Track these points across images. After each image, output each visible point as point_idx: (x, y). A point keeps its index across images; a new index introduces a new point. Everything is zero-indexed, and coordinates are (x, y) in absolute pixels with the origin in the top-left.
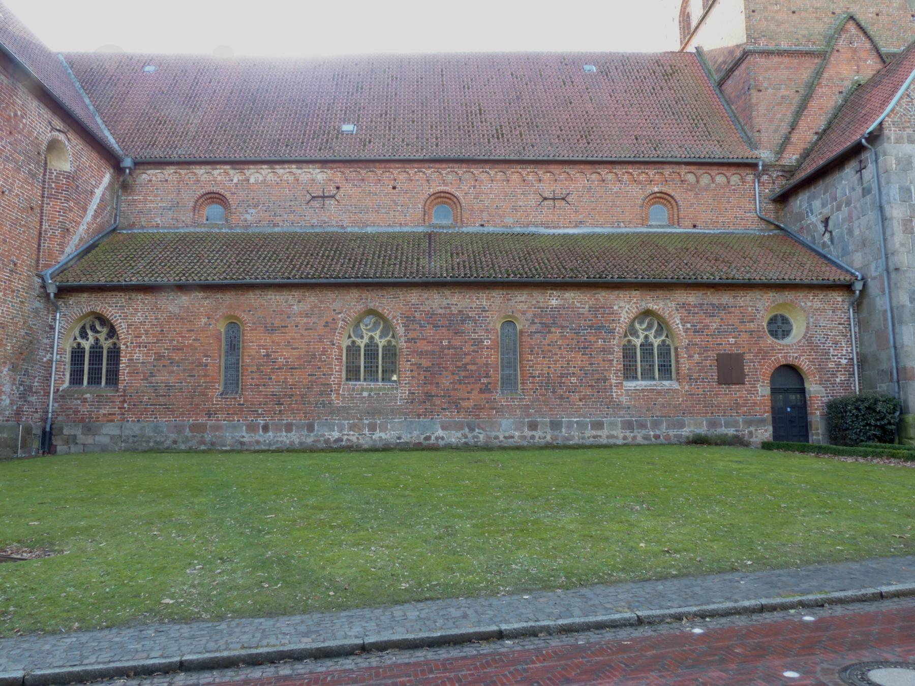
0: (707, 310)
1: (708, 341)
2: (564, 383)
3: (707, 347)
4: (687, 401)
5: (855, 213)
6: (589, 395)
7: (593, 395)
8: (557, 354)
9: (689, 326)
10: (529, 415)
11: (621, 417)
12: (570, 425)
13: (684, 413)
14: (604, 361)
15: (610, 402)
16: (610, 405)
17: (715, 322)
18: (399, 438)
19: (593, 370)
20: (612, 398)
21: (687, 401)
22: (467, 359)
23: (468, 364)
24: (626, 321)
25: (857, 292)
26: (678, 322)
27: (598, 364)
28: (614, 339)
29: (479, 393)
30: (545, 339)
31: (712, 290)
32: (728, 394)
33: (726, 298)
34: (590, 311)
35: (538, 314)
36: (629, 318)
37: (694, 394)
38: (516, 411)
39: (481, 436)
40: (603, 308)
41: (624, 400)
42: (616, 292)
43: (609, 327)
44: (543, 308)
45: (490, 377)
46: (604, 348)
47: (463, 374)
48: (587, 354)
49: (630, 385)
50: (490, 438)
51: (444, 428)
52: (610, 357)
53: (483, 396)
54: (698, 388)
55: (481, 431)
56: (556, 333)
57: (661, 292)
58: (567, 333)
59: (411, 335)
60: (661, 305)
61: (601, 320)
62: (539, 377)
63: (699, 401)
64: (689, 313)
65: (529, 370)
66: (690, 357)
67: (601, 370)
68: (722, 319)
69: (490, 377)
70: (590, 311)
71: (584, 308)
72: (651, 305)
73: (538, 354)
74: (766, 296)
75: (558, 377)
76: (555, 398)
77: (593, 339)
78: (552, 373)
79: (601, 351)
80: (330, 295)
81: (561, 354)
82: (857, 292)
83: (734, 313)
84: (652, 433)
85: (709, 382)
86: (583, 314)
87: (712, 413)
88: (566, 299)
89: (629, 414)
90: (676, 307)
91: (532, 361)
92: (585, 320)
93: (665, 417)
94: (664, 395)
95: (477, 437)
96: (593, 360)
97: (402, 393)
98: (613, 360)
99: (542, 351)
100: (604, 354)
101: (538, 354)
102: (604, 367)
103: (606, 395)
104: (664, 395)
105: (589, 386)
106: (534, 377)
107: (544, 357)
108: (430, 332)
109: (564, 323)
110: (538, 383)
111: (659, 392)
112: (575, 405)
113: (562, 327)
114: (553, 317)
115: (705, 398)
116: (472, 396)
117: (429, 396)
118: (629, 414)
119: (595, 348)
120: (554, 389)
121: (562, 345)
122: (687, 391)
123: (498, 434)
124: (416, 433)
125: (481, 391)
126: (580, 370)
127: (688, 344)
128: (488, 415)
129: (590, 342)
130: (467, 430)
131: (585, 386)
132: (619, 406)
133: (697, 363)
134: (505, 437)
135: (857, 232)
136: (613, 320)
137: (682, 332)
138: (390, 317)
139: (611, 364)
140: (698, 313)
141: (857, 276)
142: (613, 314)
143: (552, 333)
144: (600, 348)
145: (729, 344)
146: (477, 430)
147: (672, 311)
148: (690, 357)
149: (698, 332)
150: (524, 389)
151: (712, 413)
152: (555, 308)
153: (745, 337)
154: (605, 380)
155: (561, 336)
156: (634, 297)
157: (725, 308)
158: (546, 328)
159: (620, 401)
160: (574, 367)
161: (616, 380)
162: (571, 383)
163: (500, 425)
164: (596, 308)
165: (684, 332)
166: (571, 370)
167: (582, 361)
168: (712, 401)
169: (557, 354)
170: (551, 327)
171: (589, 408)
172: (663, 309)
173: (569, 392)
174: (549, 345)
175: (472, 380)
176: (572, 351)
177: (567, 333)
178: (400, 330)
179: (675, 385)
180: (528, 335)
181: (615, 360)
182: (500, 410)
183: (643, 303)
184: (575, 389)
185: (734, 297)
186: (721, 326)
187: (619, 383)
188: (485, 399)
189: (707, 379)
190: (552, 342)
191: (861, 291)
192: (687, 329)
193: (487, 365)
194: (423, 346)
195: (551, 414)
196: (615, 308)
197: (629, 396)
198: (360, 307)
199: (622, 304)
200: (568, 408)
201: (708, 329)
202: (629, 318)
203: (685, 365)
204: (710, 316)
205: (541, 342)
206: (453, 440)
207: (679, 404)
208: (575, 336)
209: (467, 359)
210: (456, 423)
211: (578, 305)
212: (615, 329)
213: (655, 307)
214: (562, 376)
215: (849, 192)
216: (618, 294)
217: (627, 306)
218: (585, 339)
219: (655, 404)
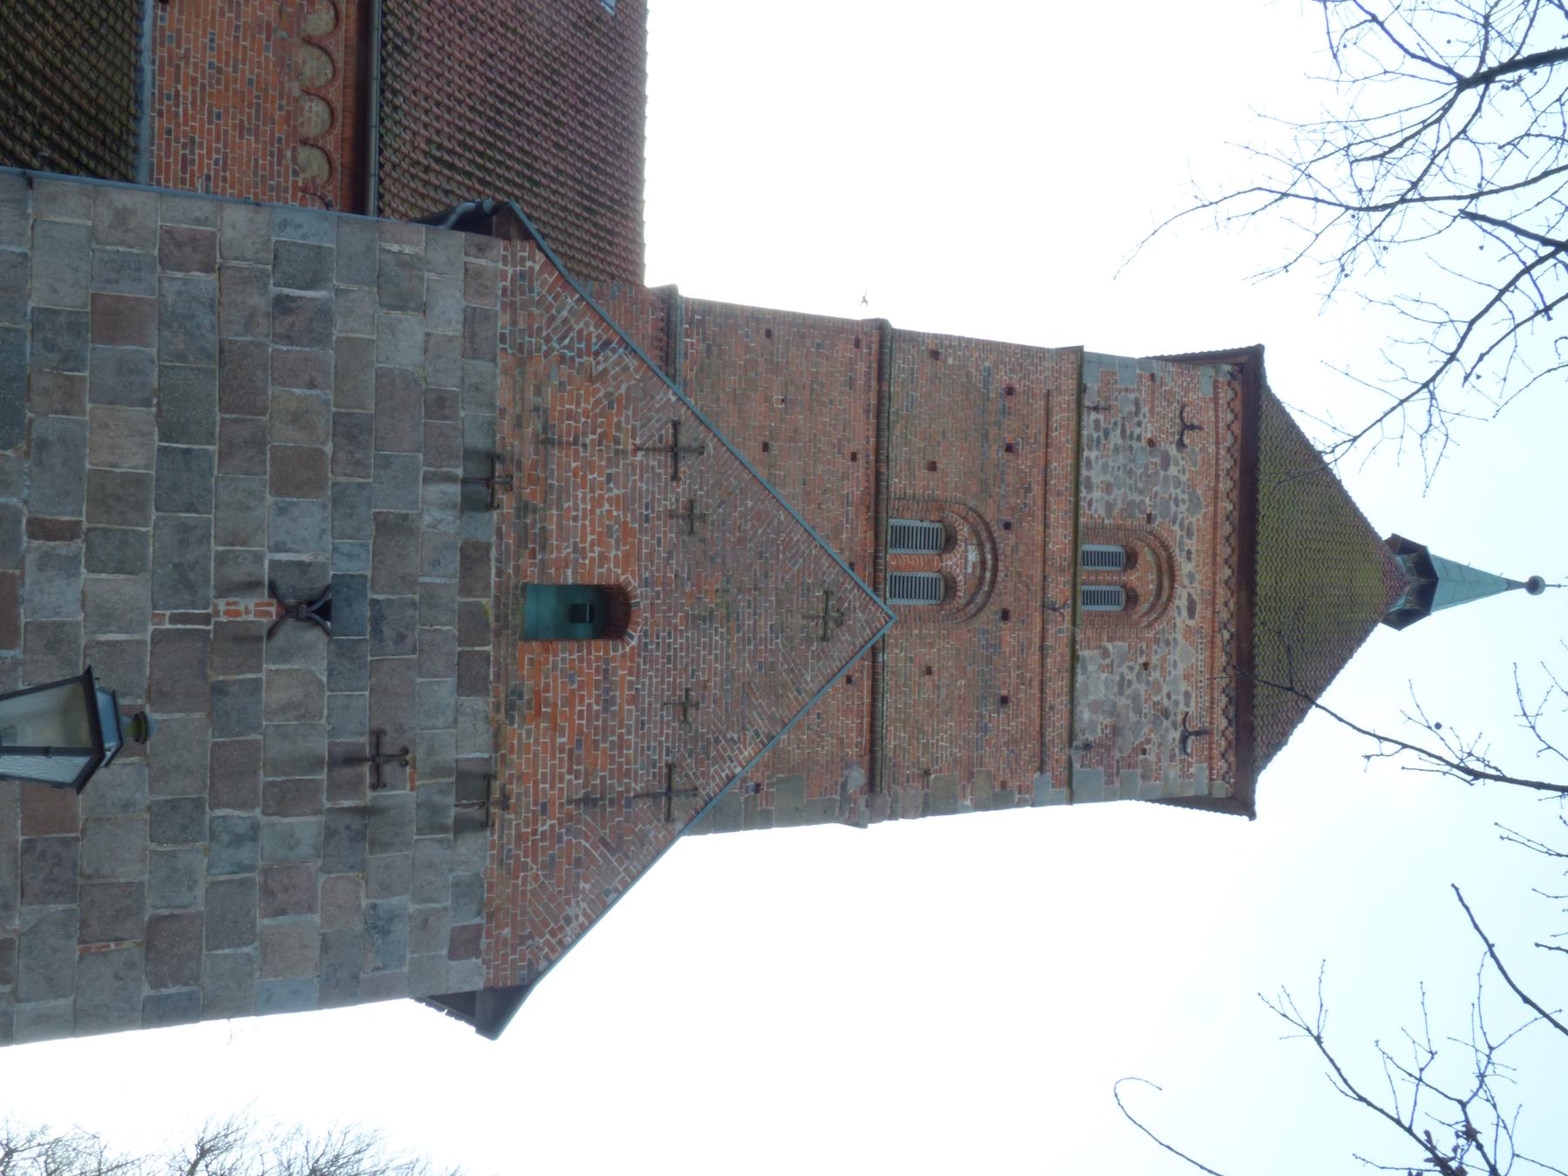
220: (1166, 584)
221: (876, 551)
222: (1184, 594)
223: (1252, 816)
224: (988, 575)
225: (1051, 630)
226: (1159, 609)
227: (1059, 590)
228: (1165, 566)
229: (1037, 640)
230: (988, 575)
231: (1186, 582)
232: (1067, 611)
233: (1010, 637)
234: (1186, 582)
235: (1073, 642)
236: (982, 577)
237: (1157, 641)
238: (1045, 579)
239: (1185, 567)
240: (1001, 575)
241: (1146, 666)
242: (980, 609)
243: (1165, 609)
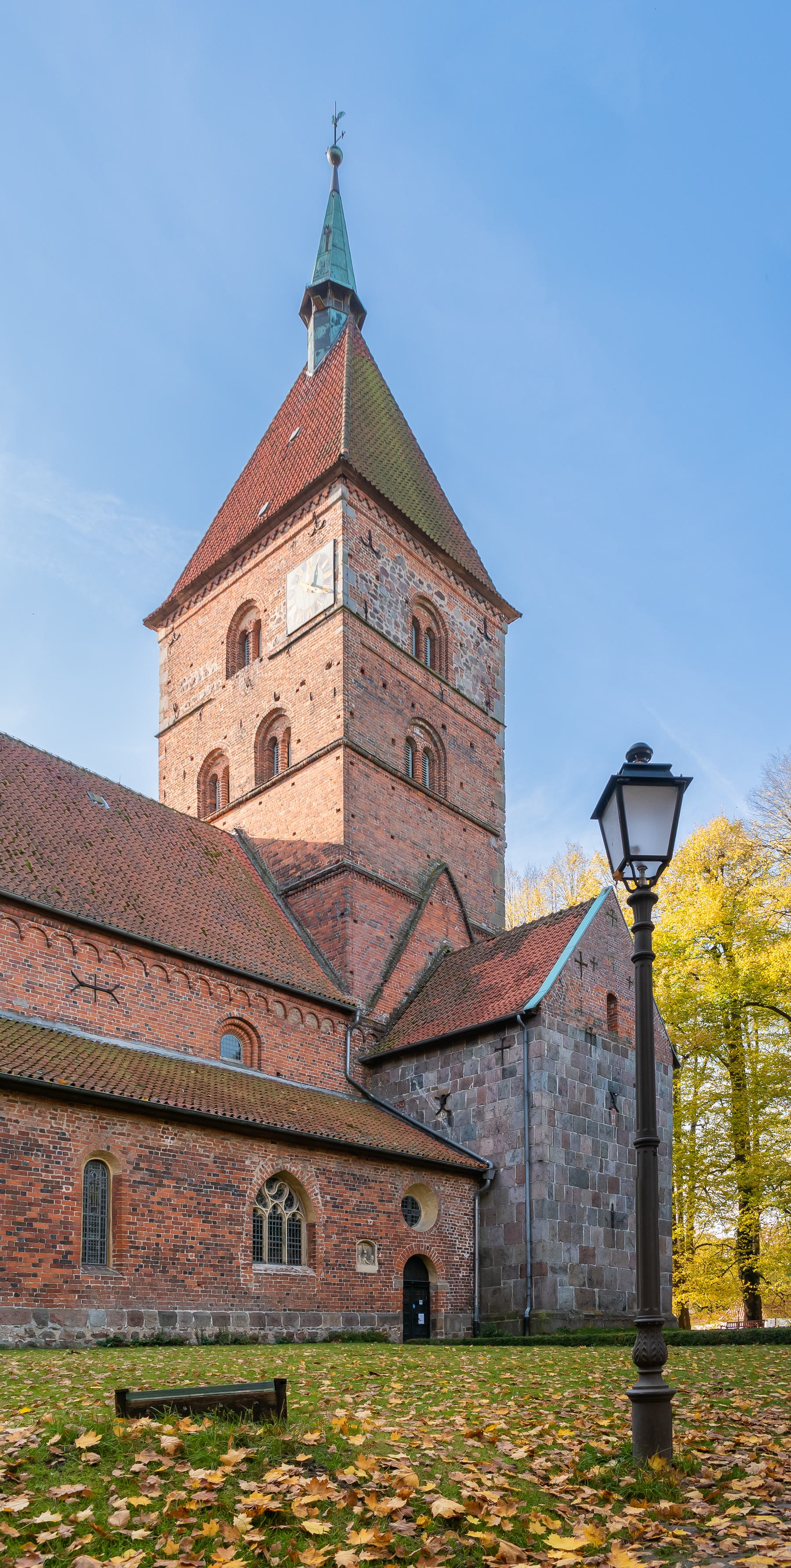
0: (347, 1181)
1: (347, 1220)
2: (178, 1259)
3: (345, 1227)
4: (322, 1291)
5: (489, 1095)
6: (210, 1278)
7: (215, 1279)
8: (170, 1218)
9: (328, 1198)
10: (128, 1304)
11: (248, 1310)
12: (186, 1319)
13: (318, 1307)
14: (230, 1233)
15: (236, 1289)
16: (236, 1293)
17: (355, 1198)
19: (216, 1245)
20: (239, 1284)
21: (322, 1291)
22: (34, 1213)
23: (35, 1220)
24: (259, 1182)
25: (489, 1181)
26: (317, 1191)
27: (223, 1236)
28: (244, 1204)
29: (52, 1266)
30: (153, 1194)
31: (354, 1157)
32: (363, 1285)
33: (367, 1170)
34: (215, 1162)
35: (146, 1156)
36: (263, 1178)
37: (330, 1284)
38: (109, 1297)
39: (57, 1334)
40: (233, 1160)
41: (253, 1286)
42: (250, 1142)
43: (238, 1187)
44: (153, 1148)
45: (71, 1243)
46: (230, 1216)
48: (209, 1222)
49: (259, 1267)
50: (69, 1335)
52: (238, 1228)
54: (334, 1277)
55: (57, 1326)
56: (169, 1186)
57: (301, 1150)
58: (185, 1189)
60: (300, 1168)
61: (228, 1177)
62: (144, 1248)
63: (335, 1292)
64: (329, 1182)
65: (130, 1237)
66: (328, 1237)
67: (227, 1245)
68: (362, 1194)
69: (71, 1243)
70: (215, 1162)
71: (208, 1157)
72: (288, 1165)
73: (143, 1215)
74: (405, 1173)
75: (170, 1250)
76: (166, 1281)
77: (217, 1201)
78: (163, 1245)
79: (227, 1220)
81: (176, 1218)
82: (489, 1181)
83: (374, 1188)
84: (285, 1331)
85: (346, 1269)
86: (207, 1165)
87: (347, 1307)
88: (185, 1140)
89: (258, 1306)
90: (316, 1173)
91: (135, 1224)
92: (209, 1175)
93: (298, 1310)
94: (299, 1283)
95: (51, 1335)
96: (218, 1232)
98: (241, 1233)
99: (150, 1211)
100: (231, 1224)
101: (143, 1215)
102: (231, 1241)
103: (231, 1279)
104: (299, 1283)
105: (211, 1266)
106: (137, 1248)
107: (151, 1221)
109: (182, 1175)
110: (142, 1257)
111: (293, 1279)
112: (193, 1291)
113: (178, 1180)
114: (168, 1165)
115: (341, 1288)
116: (40, 1271)
118: (258, 1306)
119: (221, 1215)
120: (164, 1267)
121: (177, 1205)
122: (323, 1280)
123: (83, 1330)
126: (201, 1243)
127: (327, 1221)
128: (67, 1301)
129: (214, 1205)
130: (33, 1323)
131: (206, 1266)
132: (246, 1294)
133: (335, 1245)
134: (94, 1335)
135: (489, 1116)
136: (244, 1179)
137: (320, 1205)
139: (240, 1238)
140: (338, 1184)
141: (488, 1165)
142: (244, 1170)
143: (164, 1186)
144: (226, 1215)
145: (368, 1226)
146: (50, 1325)
147: (312, 1176)
148: (328, 1237)
149: (338, 1207)
150: (121, 1265)
151: (347, 1307)
152: (170, 1151)
153: (383, 1218)
154: (232, 1259)
155: (177, 1192)
156: (271, 1152)
157: (366, 1181)
158: (157, 1179)
159: (248, 1289)
160: (193, 1238)
161: (245, 1260)
162: (189, 1260)
163: (87, 1316)
164: (224, 1159)
165: (323, 1205)
166: (189, 1242)
167: (203, 1230)
168: (347, 1292)
169: (170, 1218)
170: (163, 1177)
171: (210, 1296)
172: (302, 1172)
173: (185, 1273)
174: (159, 1203)
176: (190, 1216)
177: (185, 1189)
179: (310, 1272)
180: (130, 1186)
181: (244, 1233)
182: (85, 1295)
183: (280, 1161)
184: (194, 1269)
185: (376, 1169)
186: (361, 1202)
187: (248, 1264)
188: (62, 1276)
189: (344, 1265)
190: (163, 1199)
191: (492, 1181)
192: (327, 1202)
195: (161, 1304)
196: (247, 1162)
197: (259, 1282)
199: (256, 1159)
200: (183, 1295)
201: (347, 1204)
202: (263, 1178)
203: (322, 1245)
204: (351, 1189)
205: (148, 1197)
206: (10, 1339)
207: (315, 1295)
208: (194, 1194)
210: (16, 1313)
211: (201, 1151)
212: (246, 1192)
213: (293, 1168)
214: (175, 1249)
215: (482, 1070)
216: (252, 1145)
217: (261, 1163)
218: (208, 1200)
219: (288, 1294)
220: (428, 605)
221: (425, 793)
222: (435, 596)
223: (521, 615)
224: (430, 730)
225: (449, 701)
226: (438, 618)
227: (435, 686)
228: (421, 601)
229: (453, 713)
230: (427, 727)
231: (431, 592)
232: (444, 687)
233: (451, 730)
234: (431, 592)
235: (454, 689)
236: (426, 731)
237: (453, 631)
238: (432, 694)
239: (424, 589)
240: (430, 721)
241: (461, 645)
242: (441, 740)
243: (440, 615)
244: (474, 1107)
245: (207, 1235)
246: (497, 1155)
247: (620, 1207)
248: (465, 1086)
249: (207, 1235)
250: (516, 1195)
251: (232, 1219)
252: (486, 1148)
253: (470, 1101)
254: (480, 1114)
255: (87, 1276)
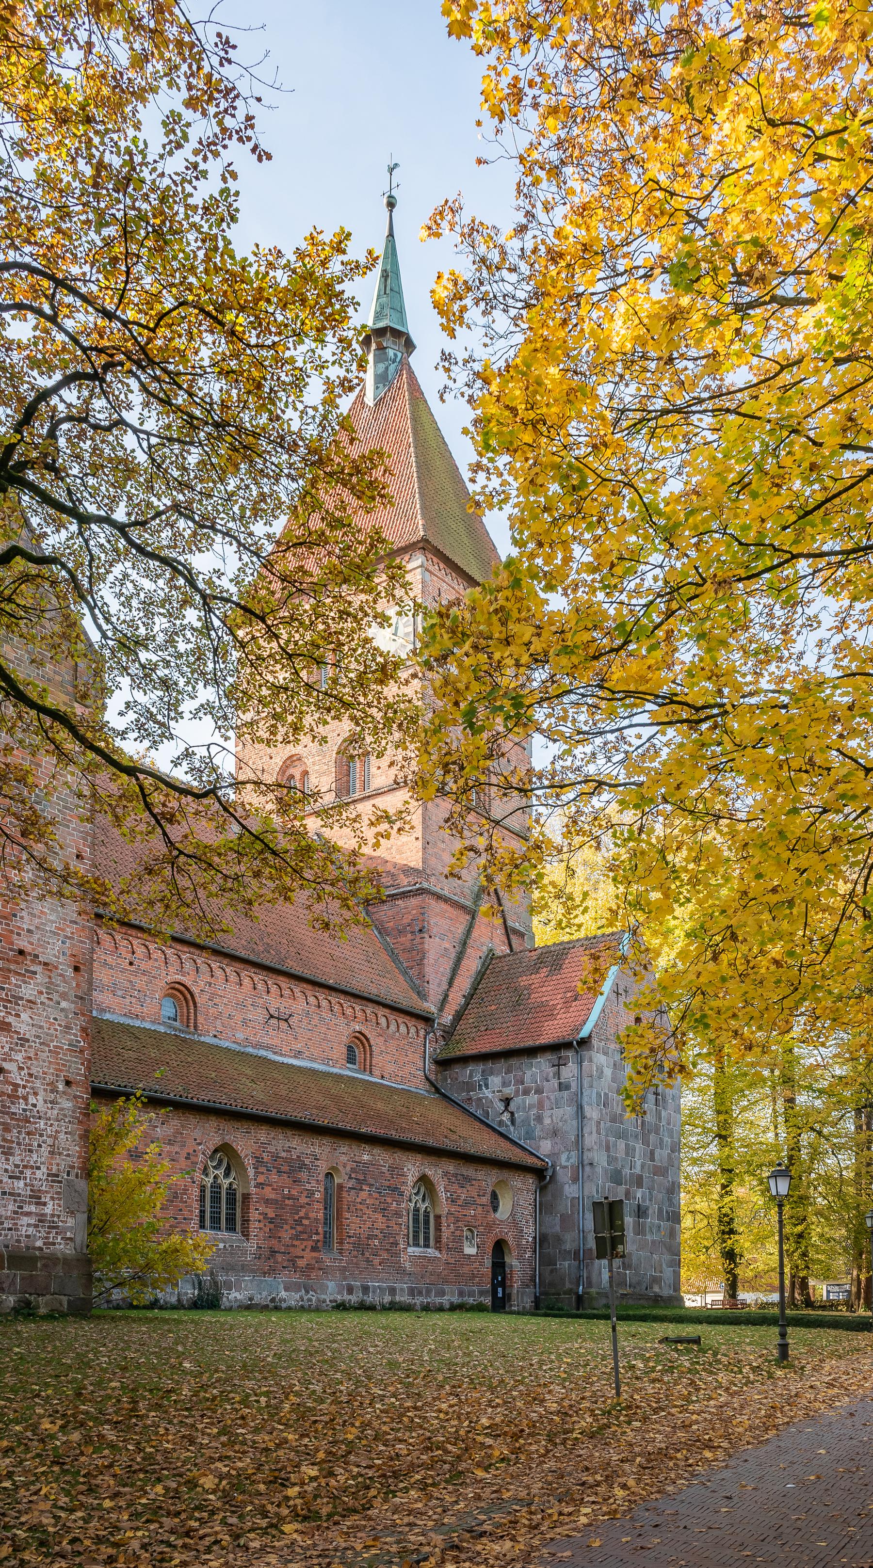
18: (251, 1299)
47: (299, 1228)
51: (286, 1289)
53: (314, 1254)
59: (261, 1179)
80: (193, 1120)
97: (251, 1246)
108: (274, 1177)
117: (273, 1252)
124: (265, 1293)
125: (314, 1249)
138: (242, 1155)
175: (305, 1236)
178: (251, 1172)
193: (316, 1219)
194: (269, 1193)
198: (217, 1141)
209: (302, 1214)
244: (534, 1111)
245: (384, 1226)
246: (554, 1155)
247: (644, 1201)
248: (526, 1092)
249: (384, 1226)
250: (570, 1190)
251: (398, 1214)
252: (545, 1147)
253: (531, 1106)
254: (539, 1119)
255: (327, 1259)
